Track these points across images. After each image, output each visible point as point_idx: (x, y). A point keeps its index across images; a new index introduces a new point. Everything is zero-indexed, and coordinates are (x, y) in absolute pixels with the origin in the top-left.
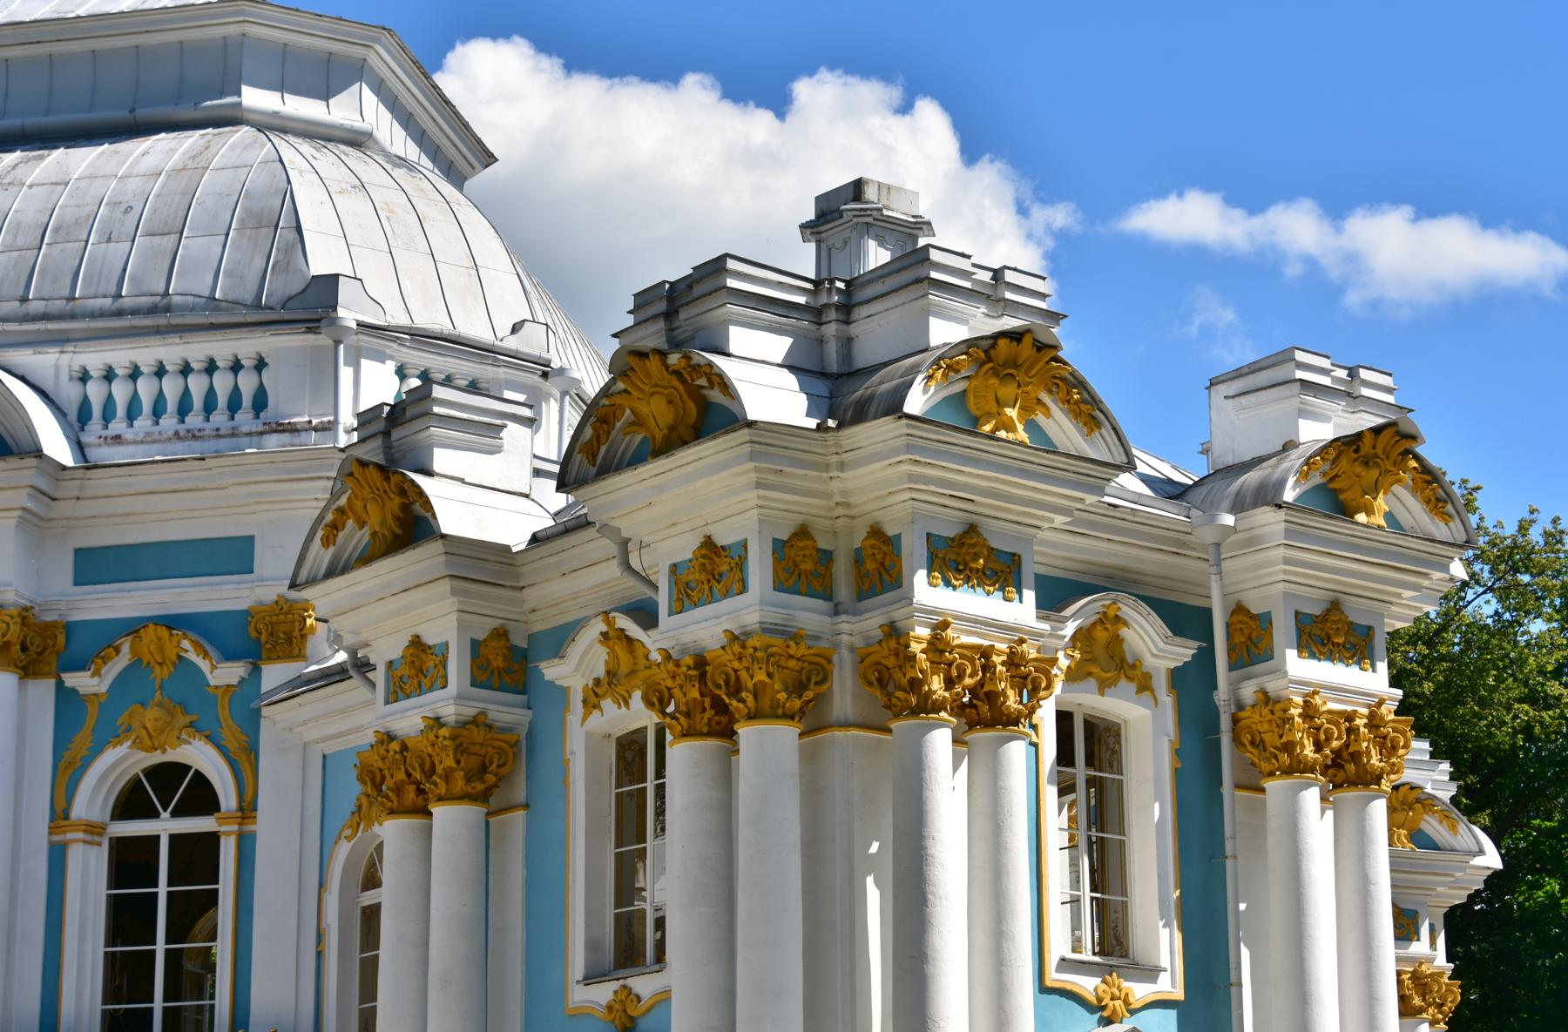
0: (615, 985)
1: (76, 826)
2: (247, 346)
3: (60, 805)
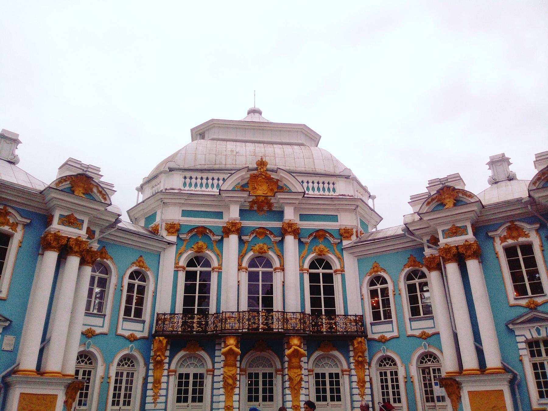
0: (529, 299)
1: (305, 270)
2: (331, 180)
3: (301, 265)
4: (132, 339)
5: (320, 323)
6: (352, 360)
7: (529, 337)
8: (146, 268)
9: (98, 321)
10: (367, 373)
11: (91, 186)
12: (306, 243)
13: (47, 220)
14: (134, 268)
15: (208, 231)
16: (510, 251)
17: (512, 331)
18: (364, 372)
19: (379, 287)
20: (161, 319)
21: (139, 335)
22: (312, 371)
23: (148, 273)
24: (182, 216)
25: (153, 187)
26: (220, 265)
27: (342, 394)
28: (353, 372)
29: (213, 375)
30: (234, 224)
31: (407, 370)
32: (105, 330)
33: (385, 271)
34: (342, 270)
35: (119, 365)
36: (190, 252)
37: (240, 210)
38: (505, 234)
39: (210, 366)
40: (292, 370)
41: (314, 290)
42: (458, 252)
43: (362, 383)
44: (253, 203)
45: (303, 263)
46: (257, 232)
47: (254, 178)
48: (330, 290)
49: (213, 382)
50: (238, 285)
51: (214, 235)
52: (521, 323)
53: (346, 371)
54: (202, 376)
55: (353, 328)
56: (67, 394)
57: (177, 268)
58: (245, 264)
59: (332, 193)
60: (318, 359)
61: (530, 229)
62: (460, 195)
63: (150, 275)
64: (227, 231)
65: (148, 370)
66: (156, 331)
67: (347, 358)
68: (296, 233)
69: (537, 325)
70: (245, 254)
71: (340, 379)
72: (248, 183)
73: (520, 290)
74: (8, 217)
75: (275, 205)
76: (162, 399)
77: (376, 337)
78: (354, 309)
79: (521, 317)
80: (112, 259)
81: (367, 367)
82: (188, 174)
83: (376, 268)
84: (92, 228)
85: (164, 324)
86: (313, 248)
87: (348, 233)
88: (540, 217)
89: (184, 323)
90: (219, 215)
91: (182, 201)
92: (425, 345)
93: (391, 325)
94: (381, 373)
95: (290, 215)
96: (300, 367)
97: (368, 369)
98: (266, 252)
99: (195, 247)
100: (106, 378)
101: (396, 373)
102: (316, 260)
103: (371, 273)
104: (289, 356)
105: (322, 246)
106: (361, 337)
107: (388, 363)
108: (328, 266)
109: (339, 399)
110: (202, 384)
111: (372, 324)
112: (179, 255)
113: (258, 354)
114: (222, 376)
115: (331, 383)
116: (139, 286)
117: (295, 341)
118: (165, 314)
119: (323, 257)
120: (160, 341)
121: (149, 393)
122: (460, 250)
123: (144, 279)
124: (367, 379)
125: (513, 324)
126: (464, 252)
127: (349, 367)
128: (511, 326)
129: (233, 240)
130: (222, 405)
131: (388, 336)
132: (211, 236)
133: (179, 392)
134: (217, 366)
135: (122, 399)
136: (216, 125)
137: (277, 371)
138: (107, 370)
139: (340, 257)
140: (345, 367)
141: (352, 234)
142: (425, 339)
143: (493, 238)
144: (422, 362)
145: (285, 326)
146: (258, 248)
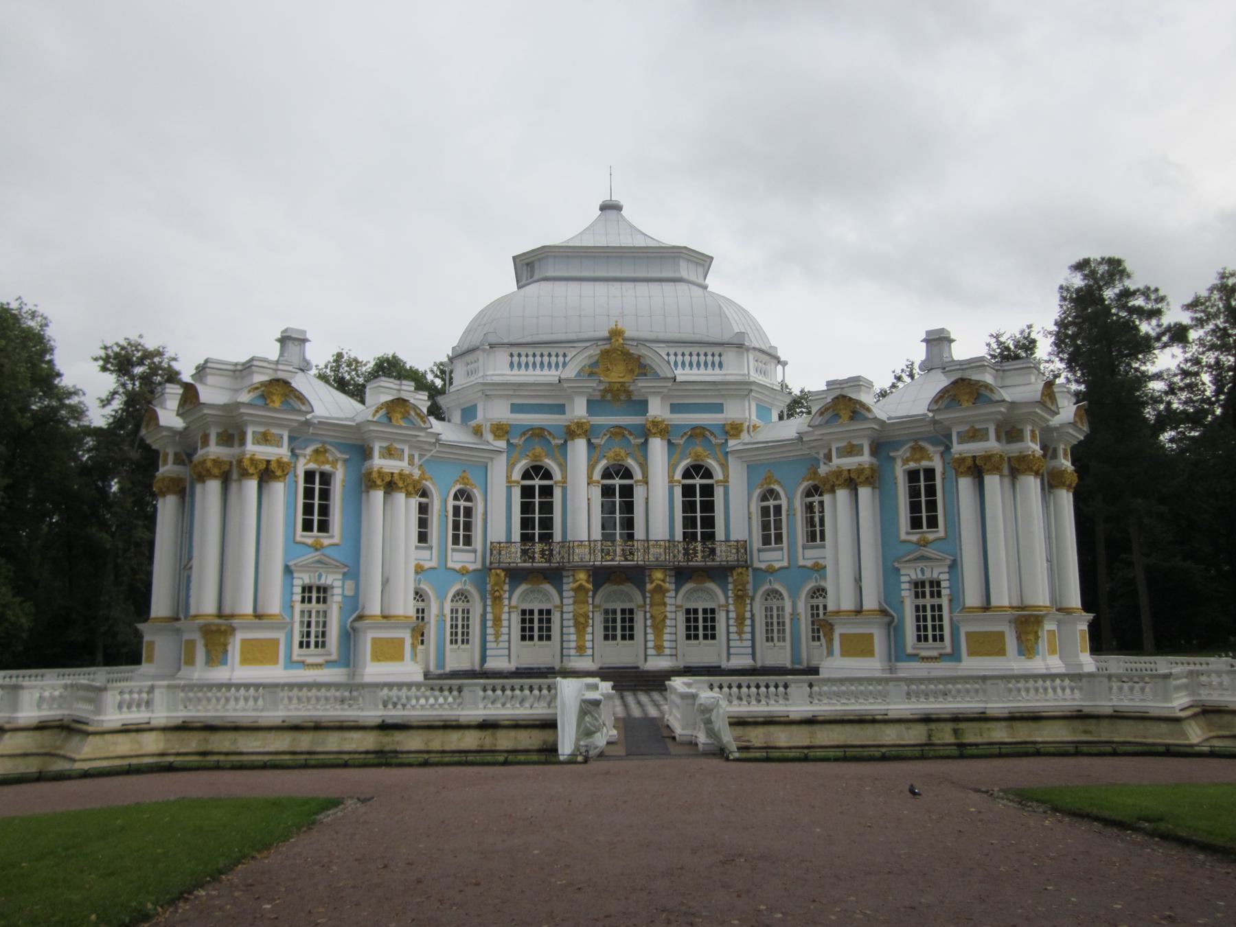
2: (717, 350)
3: (671, 474)
4: (464, 572)
5: (691, 552)
6: (730, 593)
7: (914, 577)
8: (471, 485)
9: (425, 554)
10: (748, 608)
11: (408, 408)
12: (679, 444)
13: (365, 453)
14: (458, 487)
15: (546, 433)
16: (913, 476)
17: (898, 570)
18: (745, 607)
19: (771, 503)
20: (496, 548)
21: (471, 567)
22: (681, 606)
23: (475, 491)
24: (512, 412)
25: (468, 364)
26: (565, 477)
27: (717, 632)
28: (731, 608)
29: (562, 612)
30: (580, 425)
31: (794, 606)
32: (433, 564)
33: (779, 483)
34: (726, 481)
35: (452, 601)
36: (524, 462)
37: (588, 401)
38: (908, 454)
39: (558, 602)
40: (655, 608)
41: (688, 507)
42: (850, 478)
43: (740, 620)
44: (606, 391)
45: (674, 472)
46: (611, 433)
47: (605, 354)
48: (709, 506)
49: (562, 620)
50: (589, 504)
51: (554, 438)
52: (909, 561)
53: (723, 606)
54: (549, 612)
55: (732, 557)
56: (413, 637)
57: (510, 484)
58: (597, 475)
59: (717, 371)
60: (691, 592)
61: (935, 452)
62: (858, 407)
63: (477, 493)
64: (571, 433)
65: (485, 606)
66: (491, 563)
67: (725, 592)
68: (664, 431)
69: (921, 565)
70: (597, 462)
71: (717, 616)
72: (597, 362)
73: (916, 523)
74: (327, 455)
75: (635, 393)
76: (505, 637)
77: (763, 566)
78: (738, 533)
79: (909, 554)
80: (431, 479)
81: (748, 601)
82: (515, 351)
83: (769, 479)
84: (413, 453)
85: (500, 554)
86: (687, 452)
87: (737, 429)
88: (942, 438)
89: (524, 552)
90: (560, 409)
91: (511, 393)
92: (816, 578)
93: (781, 552)
94: (766, 608)
95: (657, 409)
96: (665, 604)
97: (751, 604)
98: (623, 460)
99: (530, 454)
100: (441, 615)
101: (783, 609)
102: (692, 466)
103: (762, 485)
104: (650, 592)
105: (699, 449)
106: (743, 567)
107: (775, 597)
108: (708, 474)
109: (713, 637)
110: (549, 621)
111: (759, 551)
112: (511, 466)
113: (615, 587)
114: (571, 615)
115: (705, 620)
116: (465, 508)
117: (658, 575)
118: (500, 543)
119: (700, 463)
120: (497, 574)
121: (490, 631)
122: (853, 475)
123: (469, 499)
124: (748, 615)
125: (898, 562)
126: (856, 478)
127: (727, 602)
128: (897, 565)
129: (579, 447)
130: (573, 645)
131: (777, 565)
132: (551, 439)
133: (523, 629)
134: (565, 601)
135: (460, 638)
136: (550, 254)
137: (639, 607)
138: (442, 608)
139: (723, 462)
140: (722, 600)
141: (741, 431)
142: (818, 571)
143: (894, 459)
144: (812, 597)
145: (647, 557)
146: (613, 455)
